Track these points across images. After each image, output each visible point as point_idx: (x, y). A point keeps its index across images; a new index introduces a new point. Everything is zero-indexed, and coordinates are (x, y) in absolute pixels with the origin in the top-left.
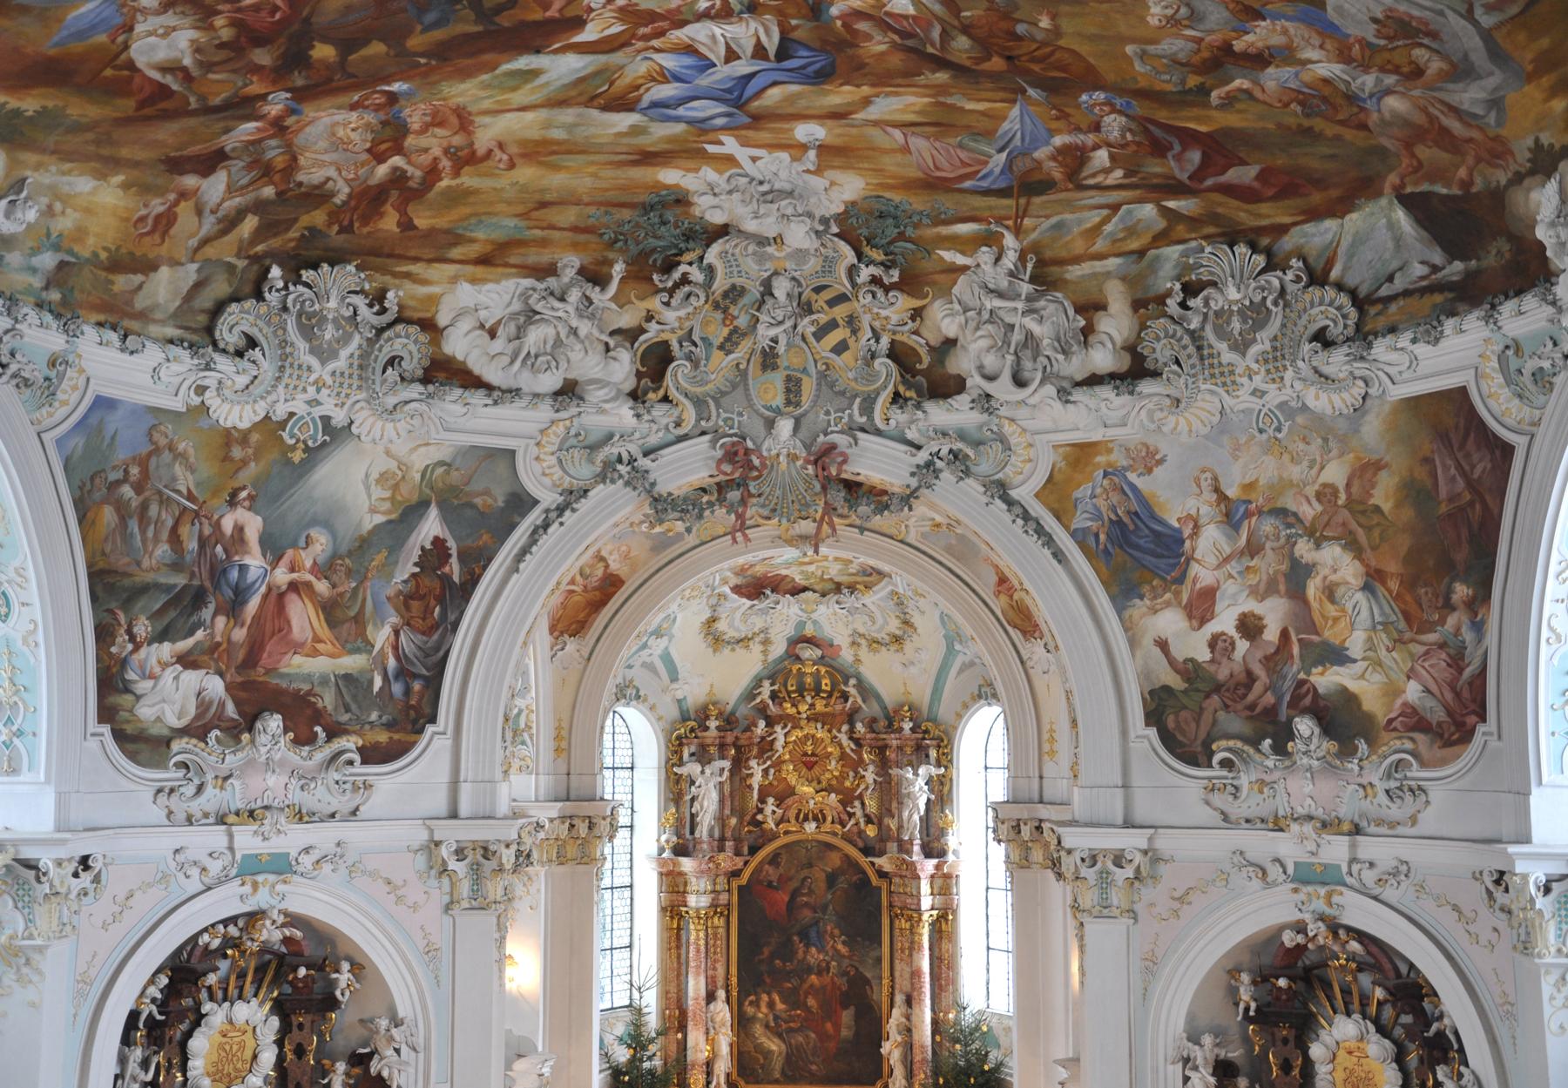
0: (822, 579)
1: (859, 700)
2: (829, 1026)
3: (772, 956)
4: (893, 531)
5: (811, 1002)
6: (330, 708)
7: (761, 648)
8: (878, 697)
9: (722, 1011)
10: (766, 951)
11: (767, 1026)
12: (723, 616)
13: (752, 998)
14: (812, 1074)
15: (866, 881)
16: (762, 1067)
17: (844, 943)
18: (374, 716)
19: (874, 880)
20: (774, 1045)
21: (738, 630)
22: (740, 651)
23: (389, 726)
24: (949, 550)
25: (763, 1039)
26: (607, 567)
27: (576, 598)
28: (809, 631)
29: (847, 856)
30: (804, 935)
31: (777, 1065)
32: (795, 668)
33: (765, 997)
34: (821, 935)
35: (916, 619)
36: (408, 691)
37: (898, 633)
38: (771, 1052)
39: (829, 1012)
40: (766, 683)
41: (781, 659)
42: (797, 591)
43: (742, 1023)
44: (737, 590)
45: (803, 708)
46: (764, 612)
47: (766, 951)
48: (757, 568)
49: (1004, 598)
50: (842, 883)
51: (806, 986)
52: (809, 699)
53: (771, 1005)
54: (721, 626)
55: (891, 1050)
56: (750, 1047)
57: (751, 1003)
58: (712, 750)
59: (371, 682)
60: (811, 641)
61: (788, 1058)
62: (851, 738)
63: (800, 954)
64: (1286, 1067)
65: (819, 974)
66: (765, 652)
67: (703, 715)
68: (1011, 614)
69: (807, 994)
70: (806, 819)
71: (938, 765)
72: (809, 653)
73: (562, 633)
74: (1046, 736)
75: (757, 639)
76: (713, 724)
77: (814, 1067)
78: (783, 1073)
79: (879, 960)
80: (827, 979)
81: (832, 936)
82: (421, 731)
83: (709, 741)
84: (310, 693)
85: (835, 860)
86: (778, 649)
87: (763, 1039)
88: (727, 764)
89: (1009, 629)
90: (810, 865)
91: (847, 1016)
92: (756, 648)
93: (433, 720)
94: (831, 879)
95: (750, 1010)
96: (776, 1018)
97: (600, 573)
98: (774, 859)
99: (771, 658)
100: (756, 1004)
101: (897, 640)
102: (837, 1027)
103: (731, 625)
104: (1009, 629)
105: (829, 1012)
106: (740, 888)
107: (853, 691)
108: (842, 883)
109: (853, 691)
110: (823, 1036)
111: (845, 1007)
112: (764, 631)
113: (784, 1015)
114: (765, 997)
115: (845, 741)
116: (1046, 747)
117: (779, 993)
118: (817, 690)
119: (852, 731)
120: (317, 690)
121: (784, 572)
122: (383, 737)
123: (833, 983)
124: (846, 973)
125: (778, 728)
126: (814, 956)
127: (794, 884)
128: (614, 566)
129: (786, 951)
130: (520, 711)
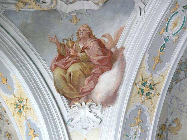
49: (59, 71)
68: (62, 85)
104: (58, 96)
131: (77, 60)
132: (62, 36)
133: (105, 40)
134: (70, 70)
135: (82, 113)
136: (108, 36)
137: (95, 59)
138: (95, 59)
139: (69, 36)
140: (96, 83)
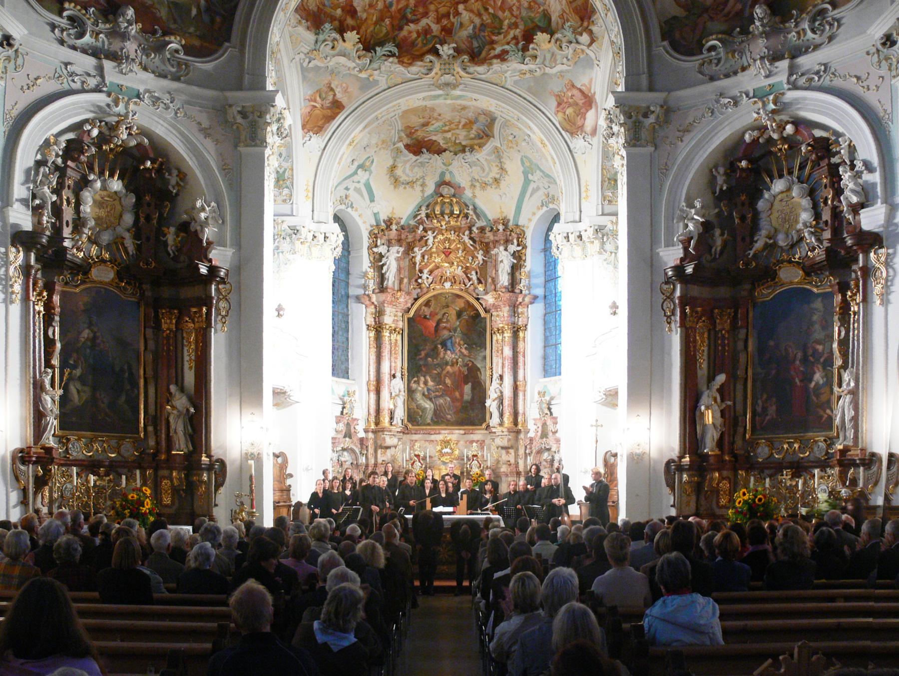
0: (455, 143)
1: (475, 217)
2: (457, 394)
3: (427, 356)
4: (498, 81)
5: (448, 381)
6: (164, 18)
7: (421, 189)
8: (485, 216)
9: (399, 384)
10: (423, 353)
11: (424, 394)
12: (400, 165)
13: (415, 379)
14: (448, 420)
15: (478, 315)
16: (421, 417)
17: (466, 348)
18: (192, 30)
19: (483, 314)
20: (428, 405)
21: (408, 176)
22: (409, 189)
23: (200, 37)
24: (529, 90)
25: (421, 402)
26: (335, 95)
27: (317, 112)
28: (447, 178)
29: (468, 302)
30: (444, 344)
31: (429, 416)
32: (439, 200)
33: (422, 379)
34: (453, 345)
35: (508, 166)
36: (212, 21)
37: (497, 176)
38: (425, 409)
39: (458, 386)
40: (423, 208)
41: (432, 196)
42: (440, 151)
43: (410, 392)
44: (407, 147)
45: (443, 223)
46: (422, 164)
47: (423, 353)
48: (419, 133)
49: (560, 115)
50: (465, 316)
51: (444, 372)
52: (446, 217)
53: (426, 383)
54: (399, 172)
55: (491, 404)
56: (414, 406)
57: (415, 382)
58: (393, 241)
59: (190, 10)
60: (448, 184)
61: (435, 411)
62: (471, 238)
63: (442, 355)
64: (743, 218)
65: (452, 365)
66: (423, 191)
67: (389, 222)
68: (565, 124)
69: (445, 376)
70: (446, 281)
71: (518, 245)
72: (445, 190)
73: (309, 131)
74: (583, 189)
75: (418, 183)
76: (394, 227)
77: (449, 417)
78: (432, 419)
79: (485, 358)
80: (456, 368)
81: (459, 345)
82: (221, 45)
83: (391, 237)
84: (152, 6)
85: (460, 304)
86: (430, 189)
87: (421, 402)
88: (401, 249)
89: (563, 132)
90: (448, 306)
91: (467, 388)
92: (418, 188)
93: (228, 40)
94: (459, 315)
95: (414, 386)
96: (428, 390)
97: (331, 98)
98: (427, 304)
99: (426, 195)
100: (417, 382)
101: (497, 181)
102: (462, 395)
103: (404, 172)
104: (563, 132)
105: (458, 386)
106: (409, 319)
107: (471, 212)
108: (465, 316)
109: (471, 212)
110: (454, 400)
111: (466, 383)
112: (423, 177)
113: (433, 388)
114: (422, 379)
115: (466, 239)
116: (583, 195)
117: (430, 376)
118: (452, 213)
119: (471, 233)
120: (157, 6)
121: (434, 138)
122: (197, 43)
123: (460, 371)
124: (467, 365)
125: (430, 233)
126: (449, 356)
127: (439, 317)
128: (339, 96)
129: (434, 352)
130: (285, 170)
131: (570, 105)
132: (556, 90)
133: (583, 88)
134: (567, 112)
135: (578, 143)
136: (584, 85)
137: (581, 102)
138: (581, 102)
139: (560, 89)
140: (585, 119)
